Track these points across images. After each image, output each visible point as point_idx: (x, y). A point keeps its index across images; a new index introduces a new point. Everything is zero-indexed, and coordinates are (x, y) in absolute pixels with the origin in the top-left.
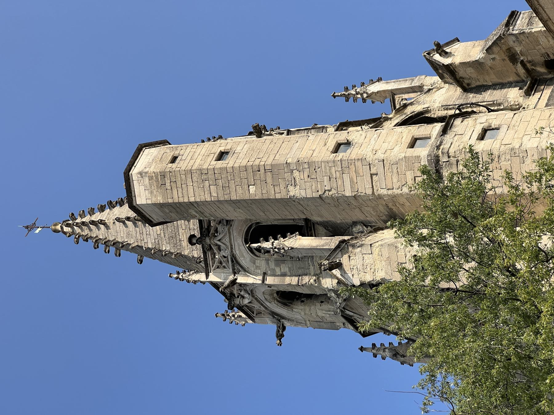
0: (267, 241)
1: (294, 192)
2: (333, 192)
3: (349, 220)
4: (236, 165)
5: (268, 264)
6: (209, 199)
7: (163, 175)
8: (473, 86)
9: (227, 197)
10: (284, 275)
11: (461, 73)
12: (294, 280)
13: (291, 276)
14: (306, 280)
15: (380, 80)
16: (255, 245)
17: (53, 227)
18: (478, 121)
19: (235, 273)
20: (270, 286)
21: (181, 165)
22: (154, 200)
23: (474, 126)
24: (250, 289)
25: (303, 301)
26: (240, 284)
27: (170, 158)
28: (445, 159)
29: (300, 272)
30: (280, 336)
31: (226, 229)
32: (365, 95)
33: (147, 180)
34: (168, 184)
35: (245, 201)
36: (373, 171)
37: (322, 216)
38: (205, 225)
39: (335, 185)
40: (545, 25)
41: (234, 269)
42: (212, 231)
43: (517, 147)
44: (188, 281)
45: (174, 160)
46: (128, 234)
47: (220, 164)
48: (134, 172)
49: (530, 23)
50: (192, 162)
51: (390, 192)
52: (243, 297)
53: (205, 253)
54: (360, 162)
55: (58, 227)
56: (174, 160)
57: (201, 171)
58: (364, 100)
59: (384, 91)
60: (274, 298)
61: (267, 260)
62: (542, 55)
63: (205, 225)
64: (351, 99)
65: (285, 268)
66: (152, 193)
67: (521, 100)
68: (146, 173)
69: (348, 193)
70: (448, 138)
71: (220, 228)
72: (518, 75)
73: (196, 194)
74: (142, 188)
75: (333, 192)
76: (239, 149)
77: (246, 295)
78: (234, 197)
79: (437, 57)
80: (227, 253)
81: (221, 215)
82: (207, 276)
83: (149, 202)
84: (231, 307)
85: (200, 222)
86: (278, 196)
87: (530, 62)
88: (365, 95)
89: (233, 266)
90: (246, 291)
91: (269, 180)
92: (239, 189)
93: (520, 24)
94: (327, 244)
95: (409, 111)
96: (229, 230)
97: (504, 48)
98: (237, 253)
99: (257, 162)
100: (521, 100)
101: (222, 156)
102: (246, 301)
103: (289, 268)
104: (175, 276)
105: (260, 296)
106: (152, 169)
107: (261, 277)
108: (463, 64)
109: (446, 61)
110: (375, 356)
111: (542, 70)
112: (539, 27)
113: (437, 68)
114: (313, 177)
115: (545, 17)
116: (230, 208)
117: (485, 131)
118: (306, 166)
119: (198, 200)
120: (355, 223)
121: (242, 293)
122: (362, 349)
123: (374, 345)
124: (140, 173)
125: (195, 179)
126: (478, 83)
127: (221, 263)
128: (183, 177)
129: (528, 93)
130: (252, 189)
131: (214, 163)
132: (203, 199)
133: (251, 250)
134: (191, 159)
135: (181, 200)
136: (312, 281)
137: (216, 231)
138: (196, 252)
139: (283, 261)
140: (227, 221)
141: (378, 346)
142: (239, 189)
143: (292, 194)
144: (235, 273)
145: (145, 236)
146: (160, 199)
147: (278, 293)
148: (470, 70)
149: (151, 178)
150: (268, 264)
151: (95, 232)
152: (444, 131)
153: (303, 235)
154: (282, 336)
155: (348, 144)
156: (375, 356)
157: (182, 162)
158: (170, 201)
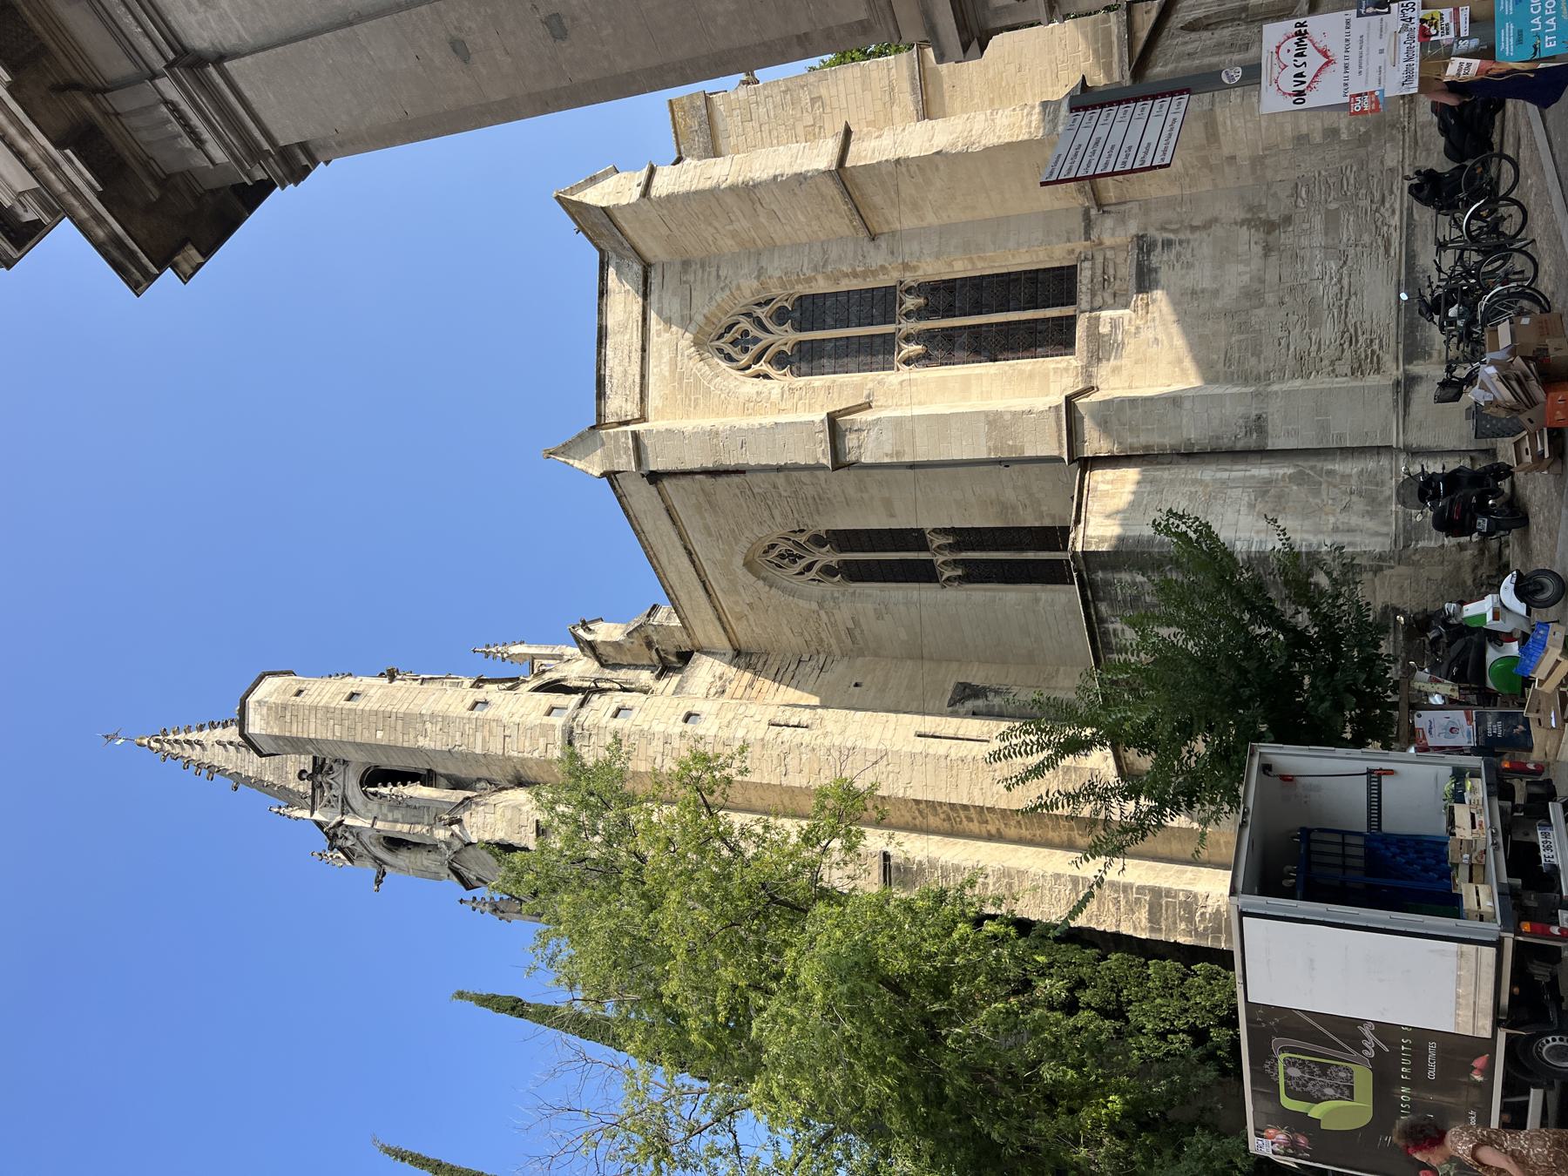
0: (385, 786)
1: (423, 742)
2: (464, 747)
3: (474, 776)
4: (367, 708)
5: (381, 808)
6: (331, 738)
7: (284, 707)
9: (351, 739)
10: (396, 821)
11: (601, 650)
12: (406, 828)
13: (403, 823)
14: (418, 828)
15: (522, 643)
16: (372, 790)
17: (139, 741)
18: (614, 700)
19: (343, 814)
20: (378, 831)
21: (305, 700)
22: (269, 731)
23: (610, 704)
24: (357, 833)
26: (347, 826)
27: (295, 691)
28: (579, 731)
29: (413, 820)
30: (379, 882)
31: (342, 768)
32: (505, 655)
33: (265, 710)
34: (288, 717)
35: (370, 744)
36: (507, 733)
37: (447, 769)
38: (319, 762)
39: (466, 742)
40: (682, 622)
41: (342, 810)
42: (326, 769)
43: (646, 729)
44: (289, 817)
45: (299, 693)
46: (227, 760)
47: (349, 705)
48: (252, 700)
49: (668, 618)
50: (319, 699)
51: (520, 755)
52: (346, 838)
53: (314, 790)
54: (495, 724)
55: (145, 742)
56: (299, 693)
57: (327, 709)
58: (504, 659)
59: (525, 654)
60: (380, 843)
62: (675, 647)
63: (319, 762)
64: (491, 656)
65: (398, 815)
66: (268, 723)
67: (651, 682)
69: (478, 751)
70: (584, 711)
71: (335, 766)
73: (318, 731)
74: (258, 717)
75: (464, 747)
76: (372, 692)
77: (351, 837)
78: (358, 740)
79: (581, 632)
80: (338, 793)
81: (341, 755)
82: (312, 813)
83: (264, 732)
84: (331, 848)
85: (315, 758)
86: (406, 745)
88: (505, 655)
89: (343, 806)
90: (351, 833)
91: (399, 727)
92: (366, 734)
93: (659, 617)
94: (447, 796)
95: (547, 677)
97: (643, 635)
98: (349, 793)
99: (389, 709)
100: (651, 682)
101: (352, 696)
102: (349, 843)
103: (403, 815)
104: (276, 810)
105: (365, 839)
106: (272, 700)
107: (371, 822)
108: (604, 642)
109: (589, 637)
110: (474, 909)
111: (673, 659)
112: (676, 622)
113: (578, 640)
115: (683, 616)
116: (353, 751)
117: (619, 710)
119: (319, 737)
120: (479, 780)
121: (347, 835)
123: (475, 898)
124: (259, 702)
125: (319, 715)
127: (329, 802)
128: (307, 712)
129: (658, 677)
130: (380, 734)
131: (342, 702)
132: (324, 737)
133: (365, 793)
134: (319, 695)
135: (300, 735)
136: (424, 830)
137: (331, 768)
138: (305, 787)
139: (397, 807)
140: (344, 761)
141: (479, 899)
142: (366, 734)
143: (420, 744)
144: (343, 814)
145: (246, 763)
146: (276, 731)
147: (385, 838)
148: (609, 649)
149: (270, 708)
150: (381, 808)
151: (188, 752)
152: (582, 704)
153: (423, 784)
154: (381, 881)
155: (486, 703)
156: (474, 909)
157: (307, 697)
158: (287, 734)
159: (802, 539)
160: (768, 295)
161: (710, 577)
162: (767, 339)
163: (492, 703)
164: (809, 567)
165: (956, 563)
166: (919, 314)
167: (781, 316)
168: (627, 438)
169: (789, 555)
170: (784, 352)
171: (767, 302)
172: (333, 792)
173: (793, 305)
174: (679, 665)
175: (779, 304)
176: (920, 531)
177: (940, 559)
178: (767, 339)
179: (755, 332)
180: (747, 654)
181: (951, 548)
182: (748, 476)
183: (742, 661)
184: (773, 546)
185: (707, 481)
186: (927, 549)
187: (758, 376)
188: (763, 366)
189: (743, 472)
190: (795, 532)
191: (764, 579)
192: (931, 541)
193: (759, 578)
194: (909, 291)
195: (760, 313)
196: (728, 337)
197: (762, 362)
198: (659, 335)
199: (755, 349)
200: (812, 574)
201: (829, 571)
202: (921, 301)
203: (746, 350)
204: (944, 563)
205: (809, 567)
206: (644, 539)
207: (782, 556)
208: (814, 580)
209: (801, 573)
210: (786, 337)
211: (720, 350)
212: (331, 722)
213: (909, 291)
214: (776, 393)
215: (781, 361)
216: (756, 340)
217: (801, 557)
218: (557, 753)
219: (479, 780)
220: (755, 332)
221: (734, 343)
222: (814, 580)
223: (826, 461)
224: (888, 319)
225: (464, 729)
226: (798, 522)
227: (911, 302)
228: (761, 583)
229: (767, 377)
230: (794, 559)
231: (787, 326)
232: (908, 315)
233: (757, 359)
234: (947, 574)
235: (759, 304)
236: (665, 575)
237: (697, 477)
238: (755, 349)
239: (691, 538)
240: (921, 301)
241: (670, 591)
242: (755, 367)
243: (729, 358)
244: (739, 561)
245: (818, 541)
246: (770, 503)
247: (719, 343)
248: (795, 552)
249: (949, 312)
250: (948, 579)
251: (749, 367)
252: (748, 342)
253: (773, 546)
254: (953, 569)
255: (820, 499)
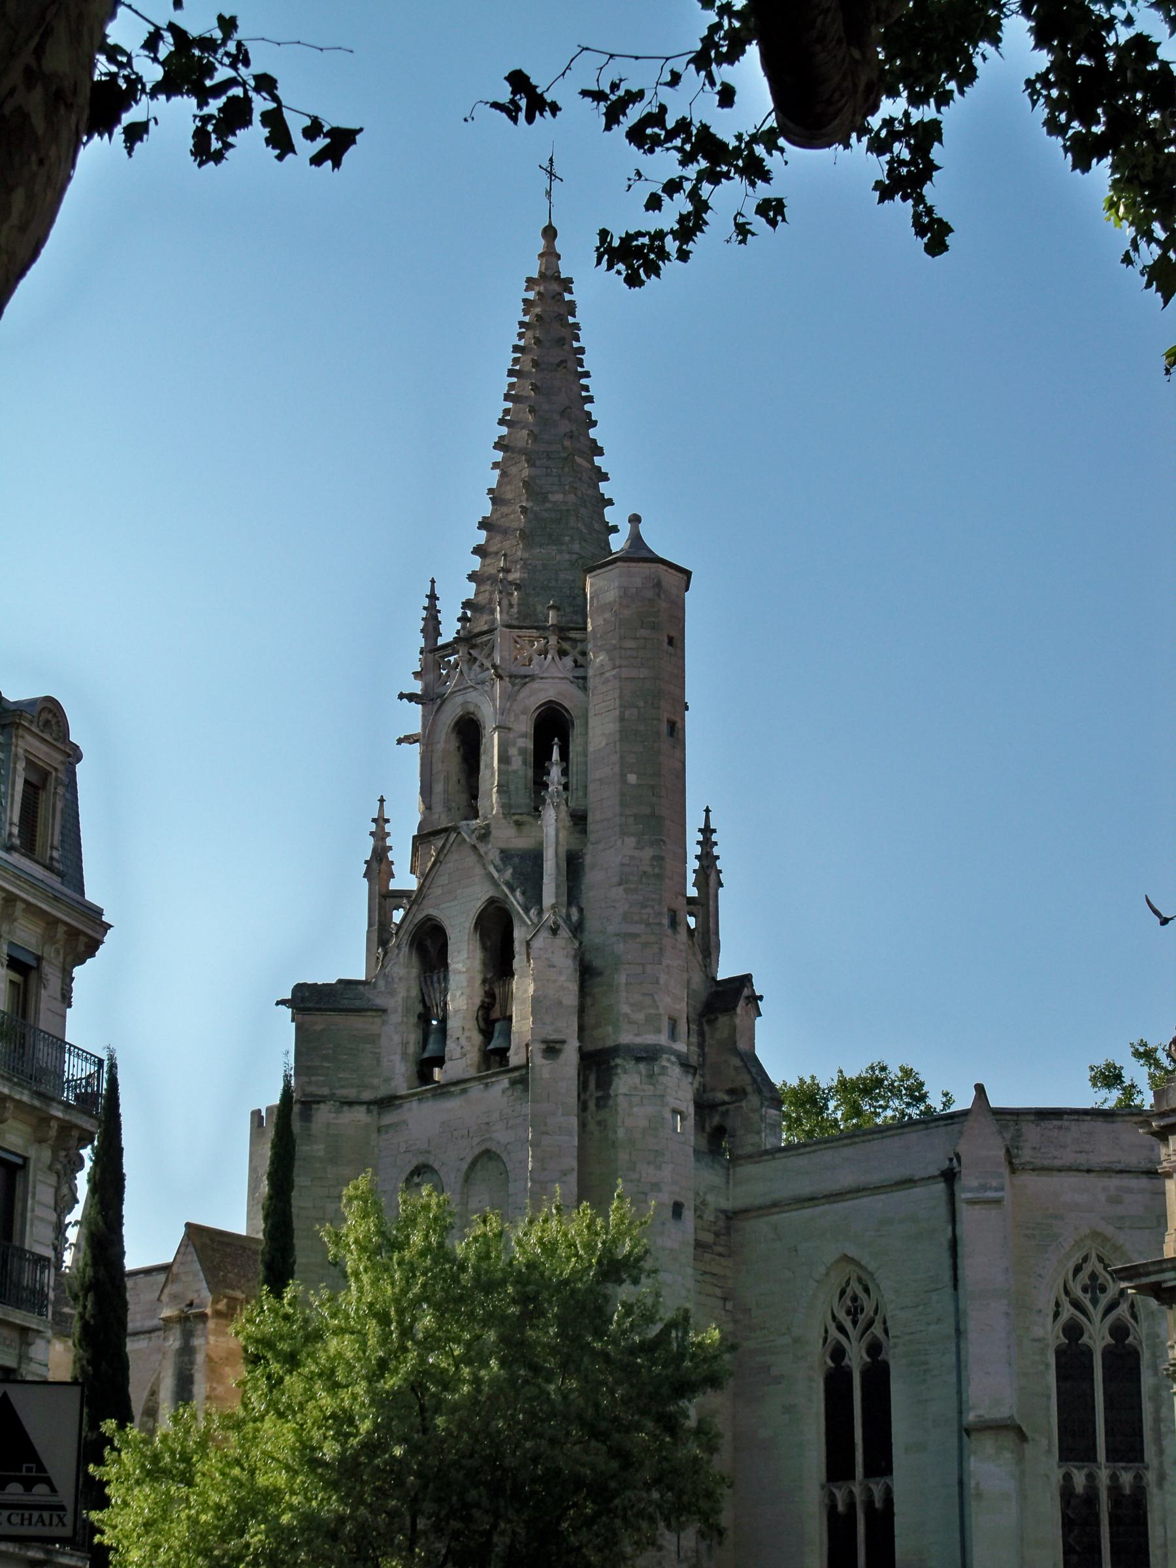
8: (706, 1028)
11: (723, 1020)
25: (459, 748)
36: (648, 967)
41: (516, 677)
42: (566, 646)
47: (664, 728)
59: (707, 894)
61: (524, 736)
68: (659, 595)
71: (568, 661)
72: (713, 1090)
79: (746, 992)
87: (727, 1111)
96: (567, 678)
97: (749, 1089)
98: (535, 685)
103: (515, 772)
108: (734, 1028)
111: (716, 1120)
114: (644, 880)
118: (657, 871)
120: (581, 910)
122: (382, 801)
124: (658, 585)
126: (708, 1036)
131: (665, 716)
159: (877, 1330)
160: (1142, 1316)
161: (827, 1207)
162: (1096, 1314)
163: (678, 936)
164: (841, 1329)
165: (851, 1506)
166: (1115, 1488)
167: (1119, 1331)
168: (996, 1190)
169: (856, 1308)
170: (1082, 1334)
171: (1134, 1316)
172: (536, 657)
173: (1130, 1345)
174: (707, 1126)
175: (1132, 1330)
176: (888, 1470)
177: (857, 1490)
178: (1096, 1314)
179: (1105, 1300)
180: (728, 1228)
181: (869, 1504)
182: (950, 1290)
183: (721, 1223)
184: (867, 1290)
185: (946, 1244)
186: (870, 1472)
187: (1057, 1305)
188: (1068, 1311)
189: (955, 1287)
190: (885, 1322)
191: (827, 1274)
192: (878, 1484)
193: (829, 1269)
194: (1138, 1477)
195: (1123, 1308)
196: (1099, 1268)
197: (1072, 1310)
198: (1104, 1189)
199: (1086, 1300)
200: (834, 1333)
201: (838, 1353)
202: (1127, 1491)
203: (1085, 1290)
204: (851, 1492)
205: (841, 1329)
206: (875, 1136)
207: (855, 1299)
208: (826, 1331)
209: (834, 1317)
210: (1097, 1337)
211: (1086, 1259)
212: (641, 704)
213: (1138, 1477)
214: (1038, 1332)
215: (1073, 1331)
216: (1095, 1302)
217: (855, 1323)
218: (626, 1038)
219: (581, 910)
220: (1105, 1300)
221: (1093, 1276)
222: (826, 1331)
223: (971, 1417)
224: (1113, 1454)
225: (646, 907)
226: (897, 1337)
227: (1126, 1478)
228: (822, 1270)
229: (1056, 1315)
230: (854, 1312)
231: (1109, 1340)
232: (1114, 1477)
233: (1076, 1304)
234: (840, 1495)
235: (1132, 1306)
236: (829, 1148)
237: (950, 1228)
238: (1086, 1300)
239: (877, 1197)
240: (1127, 1491)
241: (808, 1149)
242: (1065, 1301)
243: (1078, 1270)
244: (852, 1252)
245: (875, 1349)
246: (920, 1308)
247: (1094, 1258)
248: (861, 1317)
249: (1114, 1520)
250: (832, 1496)
251: (1067, 1293)
252: (1094, 1293)
253: (867, 1290)
254: (843, 1501)
255: (925, 1371)
